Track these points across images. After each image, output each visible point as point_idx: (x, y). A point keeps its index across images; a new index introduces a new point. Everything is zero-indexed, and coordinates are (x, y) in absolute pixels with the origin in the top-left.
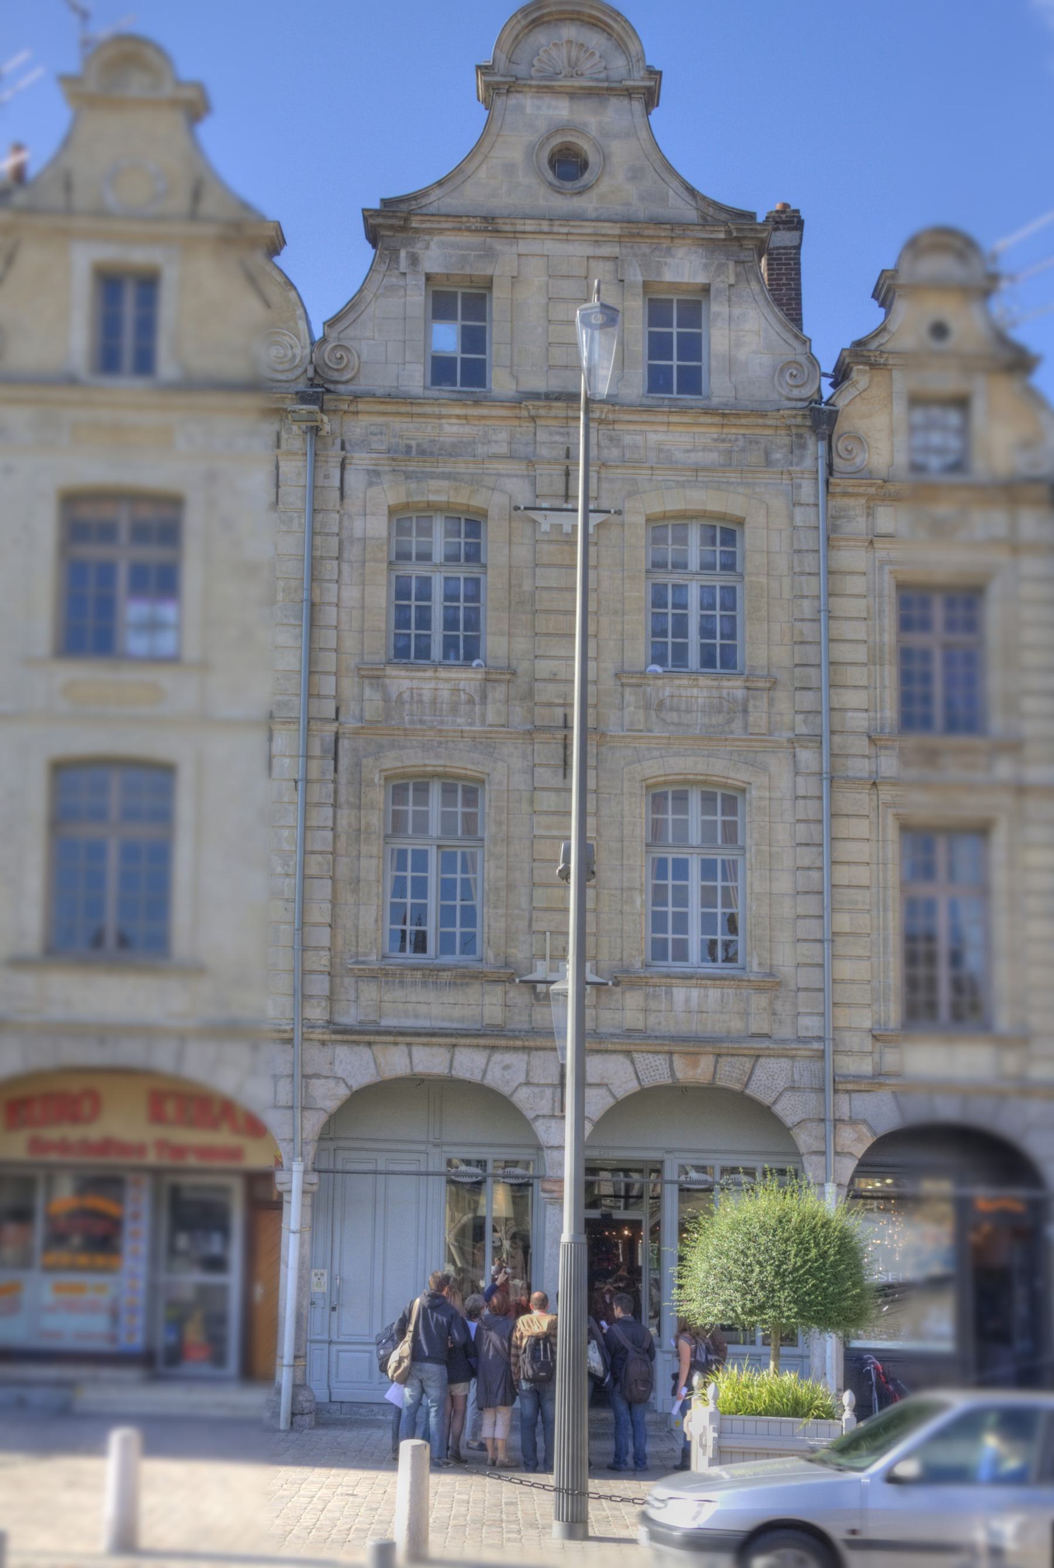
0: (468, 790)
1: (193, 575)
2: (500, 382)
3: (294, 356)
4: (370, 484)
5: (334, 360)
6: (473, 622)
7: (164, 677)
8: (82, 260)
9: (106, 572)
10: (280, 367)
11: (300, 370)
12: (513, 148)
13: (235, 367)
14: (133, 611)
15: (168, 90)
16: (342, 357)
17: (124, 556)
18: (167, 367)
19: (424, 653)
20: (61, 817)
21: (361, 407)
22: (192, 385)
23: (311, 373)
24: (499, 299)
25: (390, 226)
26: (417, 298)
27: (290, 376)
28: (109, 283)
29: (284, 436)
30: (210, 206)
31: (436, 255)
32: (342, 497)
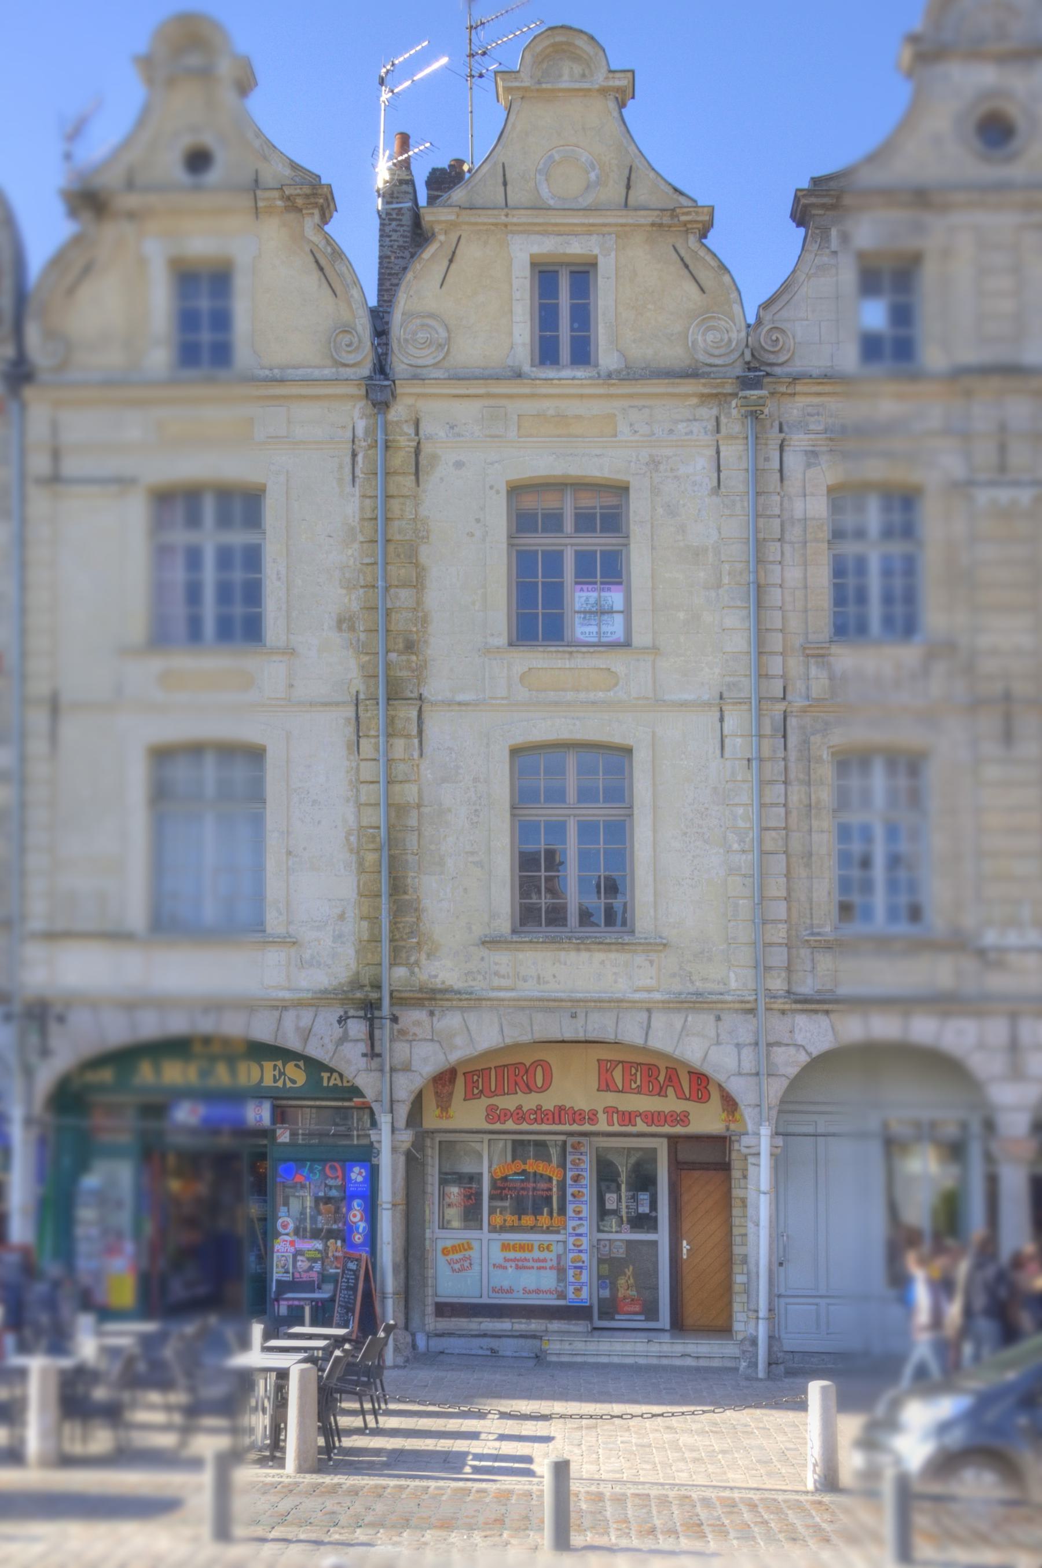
0: (909, 765)
1: (639, 562)
2: (933, 356)
3: (730, 340)
4: (809, 465)
5: (769, 342)
6: (910, 597)
7: (618, 663)
8: (523, 251)
9: (554, 560)
10: (717, 352)
11: (737, 354)
12: (944, 120)
13: (673, 355)
14: (580, 598)
15: (600, 79)
16: (777, 339)
17: (570, 545)
18: (607, 358)
19: (862, 628)
20: (522, 797)
21: (799, 388)
22: (630, 374)
23: (748, 357)
24: (930, 273)
25: (818, 206)
26: (848, 276)
27: (728, 360)
28: (544, 275)
29: (723, 420)
30: (640, 194)
31: (867, 231)
32: (782, 479)
